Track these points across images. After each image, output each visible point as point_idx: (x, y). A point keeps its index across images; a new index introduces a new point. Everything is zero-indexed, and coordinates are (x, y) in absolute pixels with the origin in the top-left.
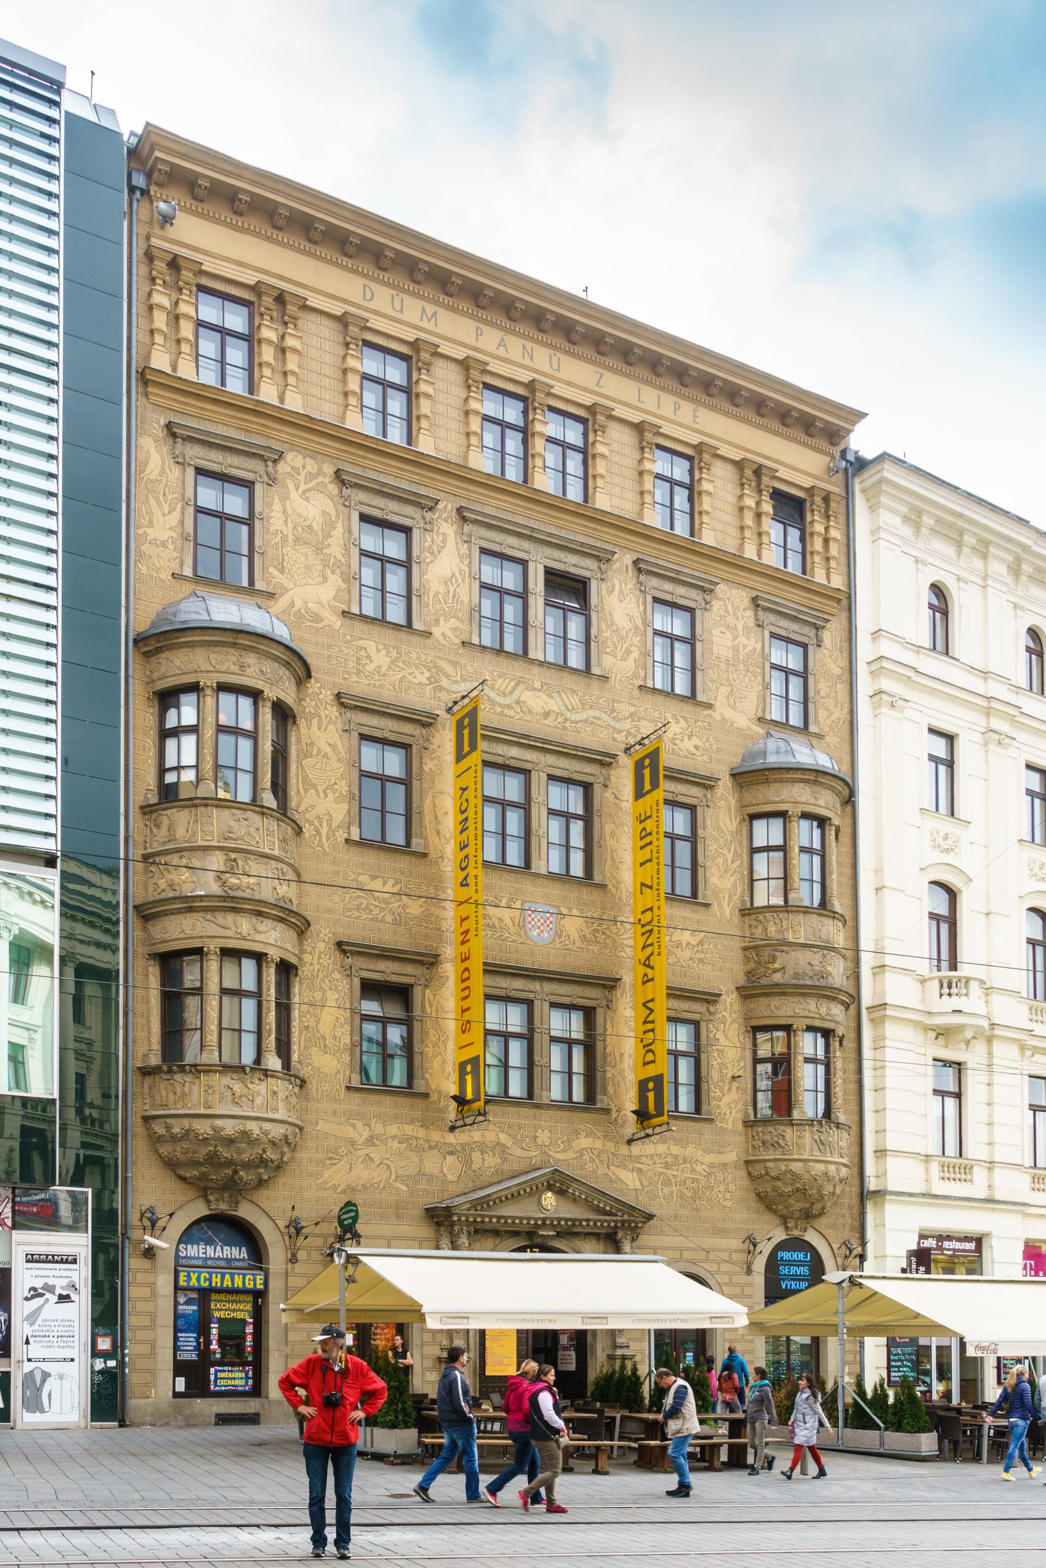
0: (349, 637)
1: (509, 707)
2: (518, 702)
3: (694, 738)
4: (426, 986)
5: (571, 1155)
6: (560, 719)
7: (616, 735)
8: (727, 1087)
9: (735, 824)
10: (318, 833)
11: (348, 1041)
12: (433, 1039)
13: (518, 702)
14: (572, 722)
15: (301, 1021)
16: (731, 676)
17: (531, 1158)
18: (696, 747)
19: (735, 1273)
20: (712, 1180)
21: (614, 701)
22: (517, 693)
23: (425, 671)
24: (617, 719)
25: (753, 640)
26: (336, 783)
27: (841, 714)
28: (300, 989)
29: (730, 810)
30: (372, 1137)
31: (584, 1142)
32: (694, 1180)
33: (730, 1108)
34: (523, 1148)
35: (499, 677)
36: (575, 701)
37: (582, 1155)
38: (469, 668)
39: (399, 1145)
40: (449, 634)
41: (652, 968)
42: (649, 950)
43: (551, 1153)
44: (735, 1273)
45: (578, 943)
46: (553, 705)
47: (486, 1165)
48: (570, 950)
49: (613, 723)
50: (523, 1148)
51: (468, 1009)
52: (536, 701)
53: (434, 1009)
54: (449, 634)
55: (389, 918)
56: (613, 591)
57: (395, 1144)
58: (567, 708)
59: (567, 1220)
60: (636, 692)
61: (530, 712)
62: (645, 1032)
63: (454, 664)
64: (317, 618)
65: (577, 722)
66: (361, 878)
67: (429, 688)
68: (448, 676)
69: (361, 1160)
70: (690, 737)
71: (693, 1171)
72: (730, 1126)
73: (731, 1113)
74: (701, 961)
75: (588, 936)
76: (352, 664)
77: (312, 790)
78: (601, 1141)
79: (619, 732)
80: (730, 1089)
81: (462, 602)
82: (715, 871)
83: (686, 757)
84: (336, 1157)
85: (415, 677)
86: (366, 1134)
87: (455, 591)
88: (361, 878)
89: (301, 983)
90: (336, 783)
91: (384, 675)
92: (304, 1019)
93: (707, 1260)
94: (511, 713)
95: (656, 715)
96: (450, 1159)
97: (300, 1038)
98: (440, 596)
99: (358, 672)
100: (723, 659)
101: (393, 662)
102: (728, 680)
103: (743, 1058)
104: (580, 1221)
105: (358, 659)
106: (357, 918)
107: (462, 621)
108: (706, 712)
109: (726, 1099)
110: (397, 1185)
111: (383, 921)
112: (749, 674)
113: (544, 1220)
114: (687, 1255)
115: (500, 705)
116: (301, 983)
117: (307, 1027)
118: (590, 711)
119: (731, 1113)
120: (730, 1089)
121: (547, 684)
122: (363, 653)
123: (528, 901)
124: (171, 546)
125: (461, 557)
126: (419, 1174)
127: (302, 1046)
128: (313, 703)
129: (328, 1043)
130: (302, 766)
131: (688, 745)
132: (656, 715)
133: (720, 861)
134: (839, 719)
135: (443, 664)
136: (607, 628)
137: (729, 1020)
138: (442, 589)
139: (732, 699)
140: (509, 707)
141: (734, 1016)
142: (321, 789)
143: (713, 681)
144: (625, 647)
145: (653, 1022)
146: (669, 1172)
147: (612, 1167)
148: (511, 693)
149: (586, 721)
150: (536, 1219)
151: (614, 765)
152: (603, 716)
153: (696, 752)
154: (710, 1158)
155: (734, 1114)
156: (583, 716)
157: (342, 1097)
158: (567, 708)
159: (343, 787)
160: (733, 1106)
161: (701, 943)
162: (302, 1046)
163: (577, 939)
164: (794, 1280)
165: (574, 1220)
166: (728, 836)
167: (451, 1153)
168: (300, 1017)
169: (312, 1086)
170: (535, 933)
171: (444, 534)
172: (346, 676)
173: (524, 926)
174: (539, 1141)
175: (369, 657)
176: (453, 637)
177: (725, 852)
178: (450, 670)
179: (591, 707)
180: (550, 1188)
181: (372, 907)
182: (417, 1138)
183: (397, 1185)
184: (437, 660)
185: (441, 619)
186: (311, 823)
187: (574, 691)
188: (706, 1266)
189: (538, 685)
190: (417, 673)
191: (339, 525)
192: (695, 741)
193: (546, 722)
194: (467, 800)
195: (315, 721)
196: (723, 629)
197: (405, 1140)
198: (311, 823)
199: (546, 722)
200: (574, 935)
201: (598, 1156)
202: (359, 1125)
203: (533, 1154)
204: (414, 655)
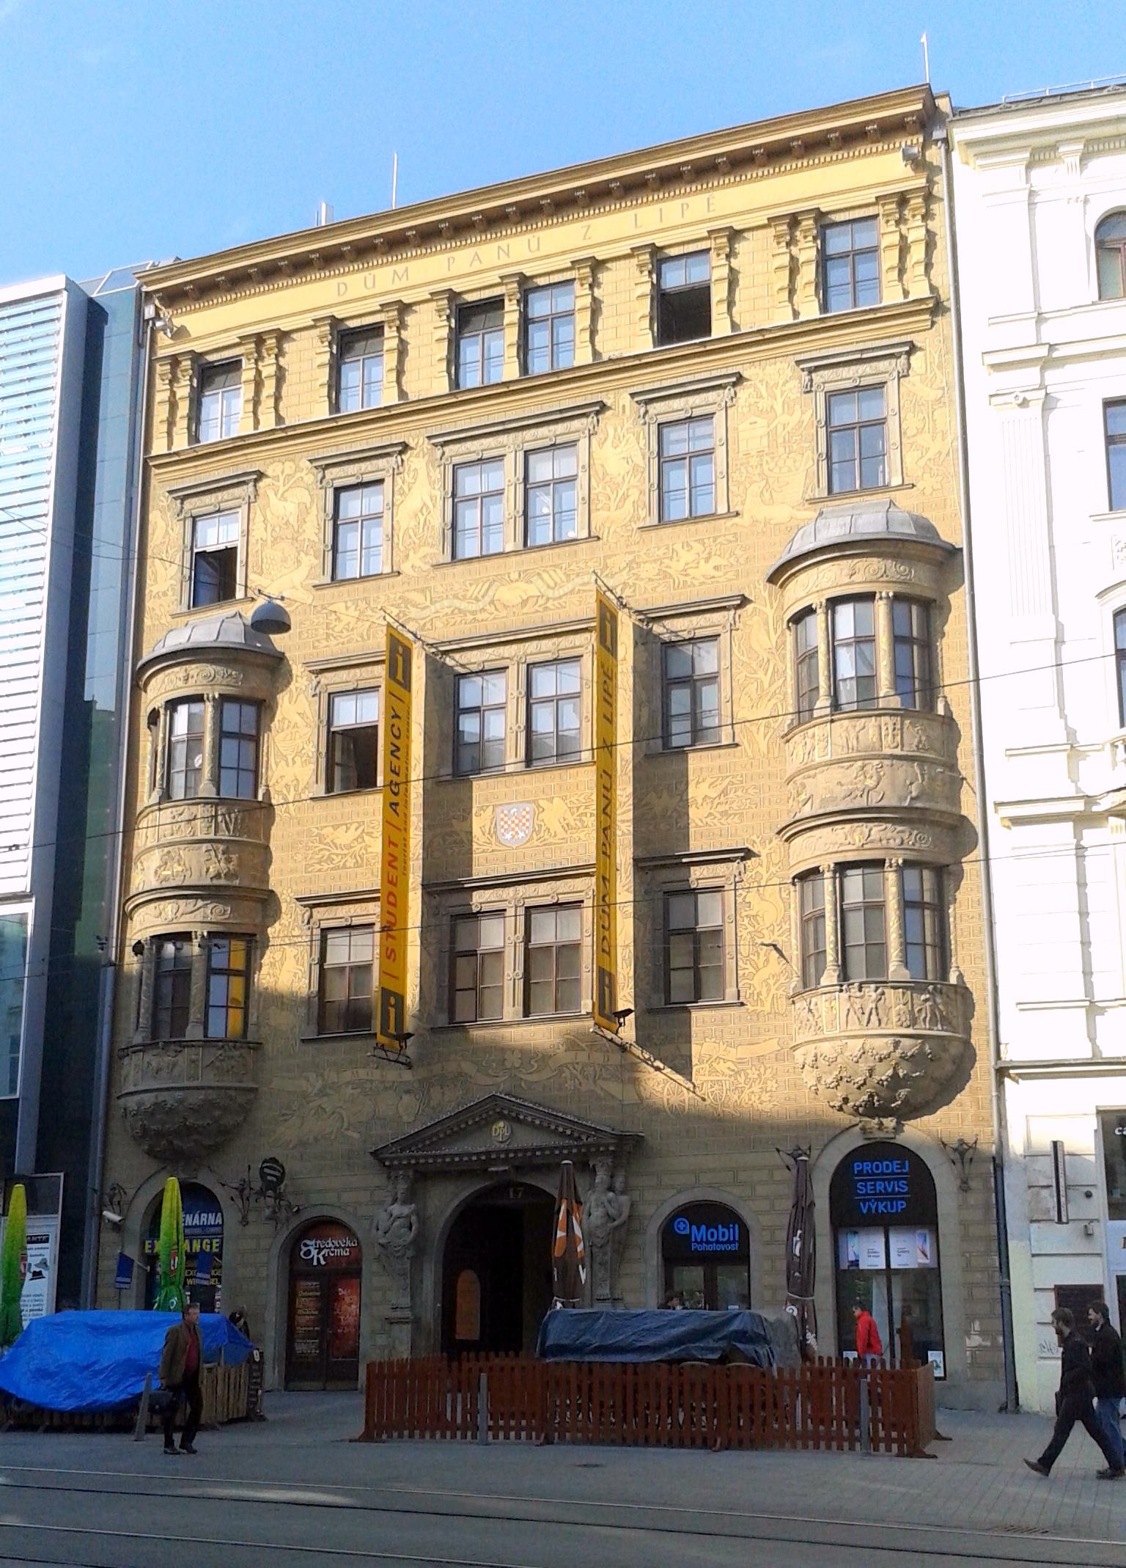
1: (483, 610)
2: (492, 602)
5: (544, 1075)
6: (540, 602)
8: (762, 958)
9: (774, 638)
14: (555, 599)
17: (498, 1085)
18: (716, 568)
20: (742, 1079)
22: (491, 593)
33: (768, 985)
34: (488, 1075)
36: (559, 575)
37: (561, 1072)
38: (440, 589)
40: (418, 563)
45: (561, 834)
46: (532, 590)
47: (446, 1098)
48: (551, 844)
50: (488, 1075)
52: (509, 594)
55: (351, 863)
57: (349, 1091)
59: (516, 1151)
60: (636, 537)
63: (423, 591)
65: (560, 597)
68: (416, 606)
72: (767, 1008)
73: (769, 991)
75: (572, 823)
76: (321, 631)
78: (586, 1054)
80: (767, 961)
82: (745, 702)
83: (701, 584)
88: (324, 831)
94: (484, 615)
96: (406, 1098)
103: (786, 918)
104: (534, 1150)
107: (433, 546)
109: (764, 973)
111: (344, 867)
113: (488, 1153)
114: (705, 1179)
115: (473, 613)
119: (769, 991)
120: (767, 961)
124: (170, 593)
125: (432, 483)
140: (483, 610)
141: (773, 869)
142: (290, 758)
144: (620, 494)
147: (600, 1082)
149: (572, 592)
150: (478, 1154)
154: (742, 1052)
155: (773, 991)
156: (570, 586)
159: (311, 749)
160: (771, 982)
161: (724, 792)
163: (560, 830)
164: (882, 1200)
165: (526, 1150)
167: (408, 1092)
169: (269, 1048)
170: (508, 836)
171: (415, 470)
174: (508, 1065)
175: (338, 619)
178: (417, 597)
179: (578, 575)
180: (502, 1117)
182: (371, 1081)
185: (411, 553)
186: (279, 793)
188: (736, 1191)
189: (514, 576)
191: (314, 507)
192: (715, 561)
193: (525, 611)
198: (279, 793)
199: (525, 611)
200: (556, 826)
201: (582, 1071)
202: (312, 1076)
203: (499, 1080)
204: (383, 598)
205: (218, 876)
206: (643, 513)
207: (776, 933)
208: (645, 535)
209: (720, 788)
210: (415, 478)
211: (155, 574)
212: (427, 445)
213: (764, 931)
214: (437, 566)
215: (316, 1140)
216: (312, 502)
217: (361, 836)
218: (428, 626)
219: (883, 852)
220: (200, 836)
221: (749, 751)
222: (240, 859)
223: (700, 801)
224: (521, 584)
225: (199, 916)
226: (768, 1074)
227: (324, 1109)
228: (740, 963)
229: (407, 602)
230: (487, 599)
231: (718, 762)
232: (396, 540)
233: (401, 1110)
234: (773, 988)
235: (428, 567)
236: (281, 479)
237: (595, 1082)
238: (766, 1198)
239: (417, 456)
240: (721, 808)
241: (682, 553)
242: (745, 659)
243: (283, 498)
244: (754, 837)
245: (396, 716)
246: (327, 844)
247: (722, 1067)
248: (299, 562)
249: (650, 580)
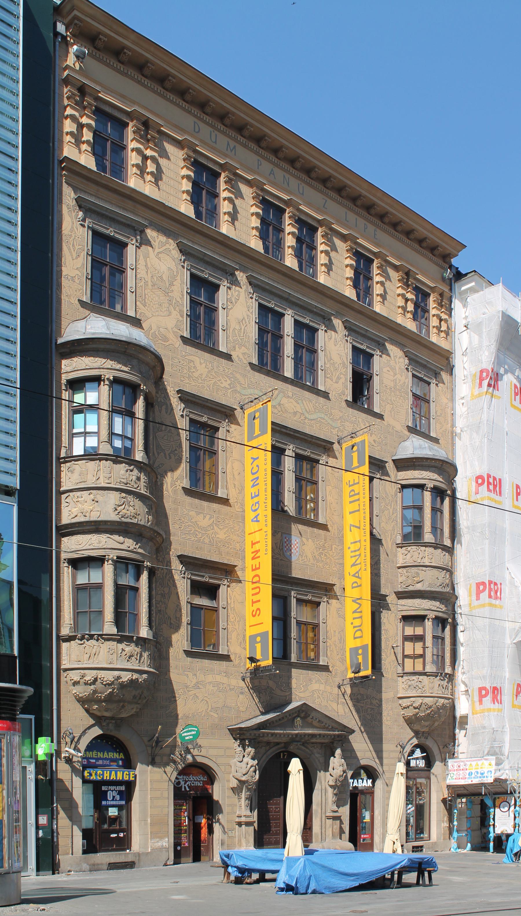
0: (184, 353)
2: (279, 404)
3: (373, 435)
4: (228, 586)
7: (332, 430)
12: (232, 620)
13: (279, 404)
15: (156, 607)
18: (374, 441)
23: (228, 380)
25: (404, 377)
26: (176, 450)
28: (156, 585)
30: (197, 682)
31: (315, 686)
33: (391, 665)
39: (213, 688)
40: (241, 356)
41: (360, 578)
42: (357, 568)
43: (297, 693)
45: (312, 561)
49: (331, 422)
51: (259, 601)
53: (232, 601)
54: (241, 356)
56: (331, 338)
57: (211, 688)
60: (344, 404)
62: (354, 619)
66: (190, 513)
67: (230, 391)
68: (240, 384)
69: (191, 697)
71: (371, 704)
73: (391, 668)
76: (185, 371)
77: (162, 454)
79: (334, 428)
81: (249, 336)
85: (222, 383)
86: (194, 681)
87: (244, 329)
88: (190, 513)
89: (156, 582)
90: (176, 450)
91: (204, 380)
92: (158, 605)
95: (354, 419)
97: (156, 618)
98: (236, 331)
99: (189, 377)
100: (388, 387)
101: (209, 372)
105: (189, 368)
110: (212, 713)
112: (401, 398)
116: (156, 582)
117: (160, 611)
118: (318, 414)
119: (391, 668)
121: (295, 394)
122: (192, 364)
123: (285, 533)
127: (157, 623)
128: (163, 395)
129: (172, 622)
130: (155, 436)
132: (354, 419)
135: (238, 376)
136: (328, 361)
138: (237, 327)
142: (167, 453)
144: (337, 374)
145: (361, 612)
146: (359, 704)
151: (331, 449)
152: (326, 418)
153: (374, 444)
155: (392, 669)
157: (180, 657)
158: (306, 411)
160: (392, 664)
162: (157, 623)
167: (242, 693)
168: (156, 604)
172: (182, 379)
173: (282, 549)
175: (195, 367)
176: (243, 359)
177: (389, 508)
181: (197, 533)
183: (212, 713)
184: (234, 373)
185: (237, 346)
187: (310, 401)
189: (290, 394)
190: (223, 382)
193: (295, 419)
194: (258, 466)
195: (164, 407)
196: (388, 369)
199: (295, 419)
202: (190, 675)
217: (211, 525)
224: (296, 404)
233: (239, 705)
234: (392, 667)
235: (245, 362)
237: (327, 702)
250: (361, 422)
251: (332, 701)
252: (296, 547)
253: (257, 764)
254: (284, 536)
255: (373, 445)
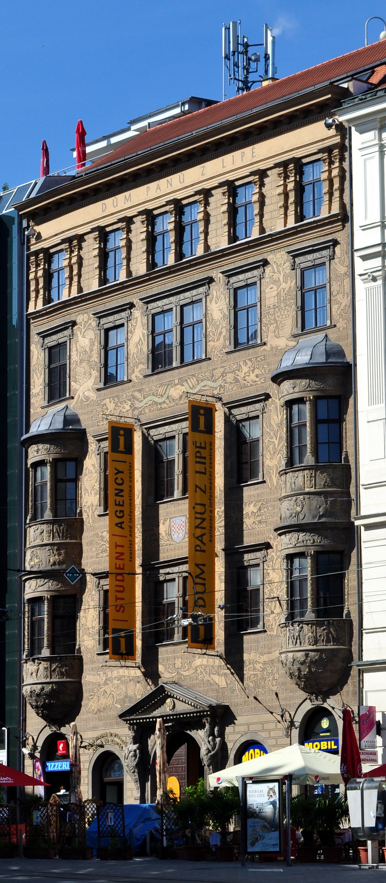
2: (168, 398)
8: (274, 605)
9: (280, 417)
10: (88, 515)
11: (97, 628)
16: (276, 315)
19: (280, 737)
20: (265, 673)
21: (214, 370)
22: (167, 392)
24: (215, 381)
27: (346, 301)
29: (277, 408)
30: (106, 680)
32: (255, 675)
33: (275, 620)
35: (159, 387)
36: (194, 381)
37: (197, 670)
40: (138, 375)
44: (280, 737)
57: (116, 682)
58: (190, 388)
60: (225, 357)
61: (173, 400)
63: (140, 391)
64: (87, 398)
68: (137, 400)
70: (253, 372)
71: (254, 669)
72: (275, 633)
74: (260, 522)
83: (251, 385)
84: (93, 694)
86: (104, 678)
93: (263, 730)
96: (138, 685)
102: (275, 319)
106: (102, 557)
108: (262, 349)
121: (181, 378)
122: (105, 407)
123: (173, 518)
125: (143, 326)
126: (125, 697)
131: (253, 376)
133: (271, 446)
134: (346, 306)
137: (275, 558)
139: (277, 331)
140: (164, 402)
142: (89, 491)
143: (266, 325)
147: (211, 675)
148: (164, 394)
159: (97, 486)
160: (277, 618)
161: (260, 509)
166: (276, 428)
167: (139, 682)
173: (171, 534)
177: (274, 440)
179: (202, 381)
189: (177, 382)
192: (257, 372)
193: (181, 402)
197: (119, 678)
199: (181, 402)
201: (205, 669)
205: (54, 564)
206: (228, 343)
207: (279, 591)
208: (229, 356)
209: (258, 507)
210: (136, 323)
211: (34, 382)
212: (141, 303)
213: (275, 590)
214: (146, 376)
215: (104, 709)
216: (95, 338)
218: (143, 412)
219: (304, 548)
220: (45, 542)
221: (270, 485)
222: (66, 553)
223: (250, 514)
225: (45, 588)
226: (275, 671)
227: (106, 692)
228: (265, 608)
229: (134, 397)
230: (166, 396)
231: (257, 492)
232: (129, 360)
235: (141, 377)
236: (83, 323)
238: (274, 738)
239: (137, 310)
240: (259, 518)
241: (243, 367)
242: (268, 430)
243: (84, 337)
244: (271, 536)
245: (119, 472)
246: (104, 542)
247: (258, 666)
248: (91, 374)
249: (231, 383)
250: (242, 365)
251: (215, 674)
252: (182, 527)
253: (138, 748)
254: (172, 520)
255: (256, 381)
